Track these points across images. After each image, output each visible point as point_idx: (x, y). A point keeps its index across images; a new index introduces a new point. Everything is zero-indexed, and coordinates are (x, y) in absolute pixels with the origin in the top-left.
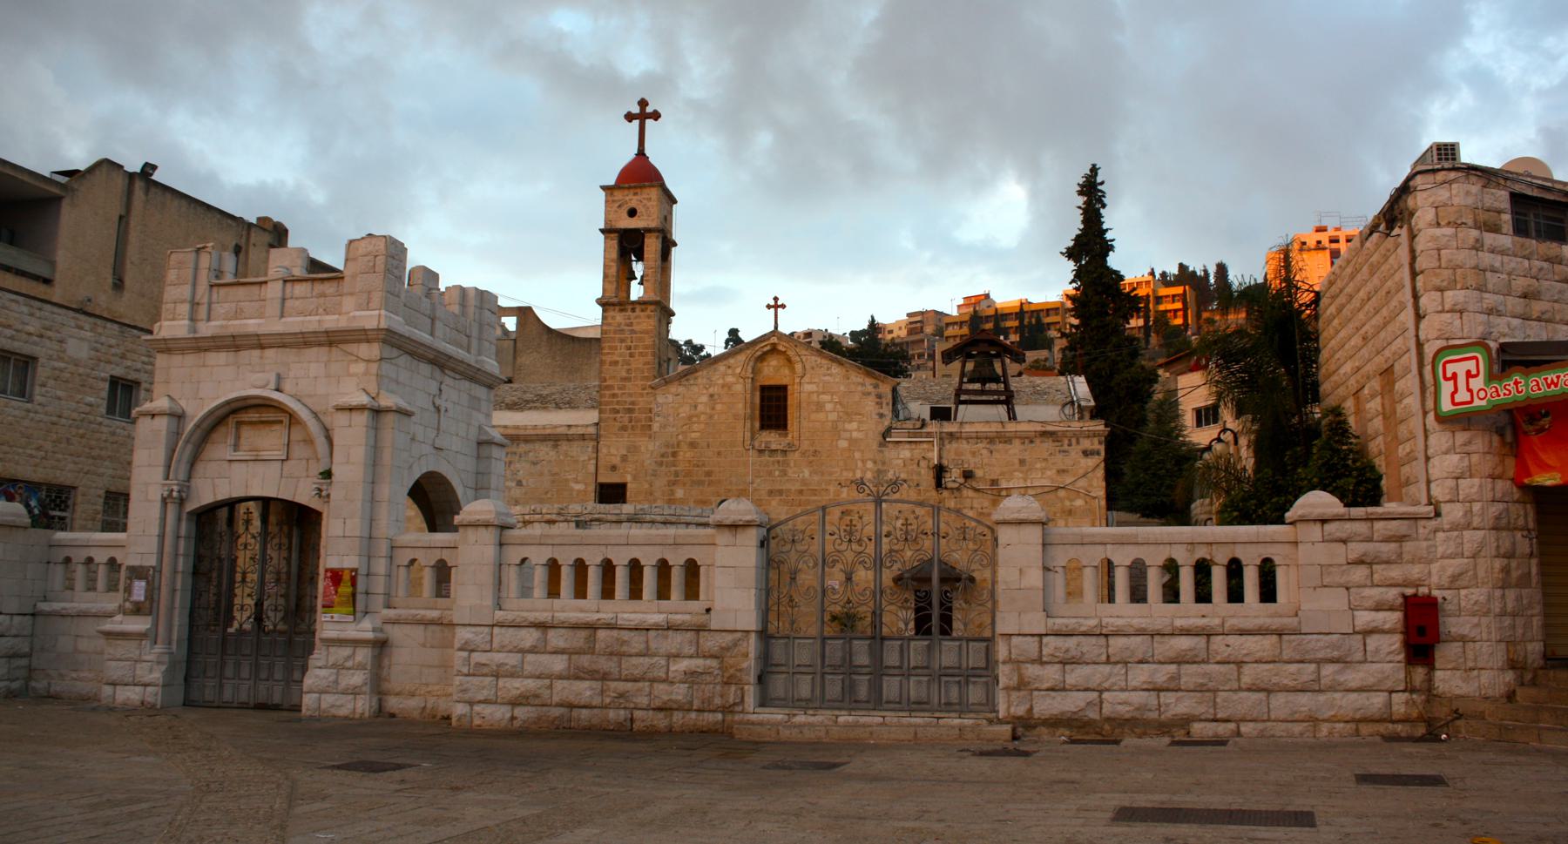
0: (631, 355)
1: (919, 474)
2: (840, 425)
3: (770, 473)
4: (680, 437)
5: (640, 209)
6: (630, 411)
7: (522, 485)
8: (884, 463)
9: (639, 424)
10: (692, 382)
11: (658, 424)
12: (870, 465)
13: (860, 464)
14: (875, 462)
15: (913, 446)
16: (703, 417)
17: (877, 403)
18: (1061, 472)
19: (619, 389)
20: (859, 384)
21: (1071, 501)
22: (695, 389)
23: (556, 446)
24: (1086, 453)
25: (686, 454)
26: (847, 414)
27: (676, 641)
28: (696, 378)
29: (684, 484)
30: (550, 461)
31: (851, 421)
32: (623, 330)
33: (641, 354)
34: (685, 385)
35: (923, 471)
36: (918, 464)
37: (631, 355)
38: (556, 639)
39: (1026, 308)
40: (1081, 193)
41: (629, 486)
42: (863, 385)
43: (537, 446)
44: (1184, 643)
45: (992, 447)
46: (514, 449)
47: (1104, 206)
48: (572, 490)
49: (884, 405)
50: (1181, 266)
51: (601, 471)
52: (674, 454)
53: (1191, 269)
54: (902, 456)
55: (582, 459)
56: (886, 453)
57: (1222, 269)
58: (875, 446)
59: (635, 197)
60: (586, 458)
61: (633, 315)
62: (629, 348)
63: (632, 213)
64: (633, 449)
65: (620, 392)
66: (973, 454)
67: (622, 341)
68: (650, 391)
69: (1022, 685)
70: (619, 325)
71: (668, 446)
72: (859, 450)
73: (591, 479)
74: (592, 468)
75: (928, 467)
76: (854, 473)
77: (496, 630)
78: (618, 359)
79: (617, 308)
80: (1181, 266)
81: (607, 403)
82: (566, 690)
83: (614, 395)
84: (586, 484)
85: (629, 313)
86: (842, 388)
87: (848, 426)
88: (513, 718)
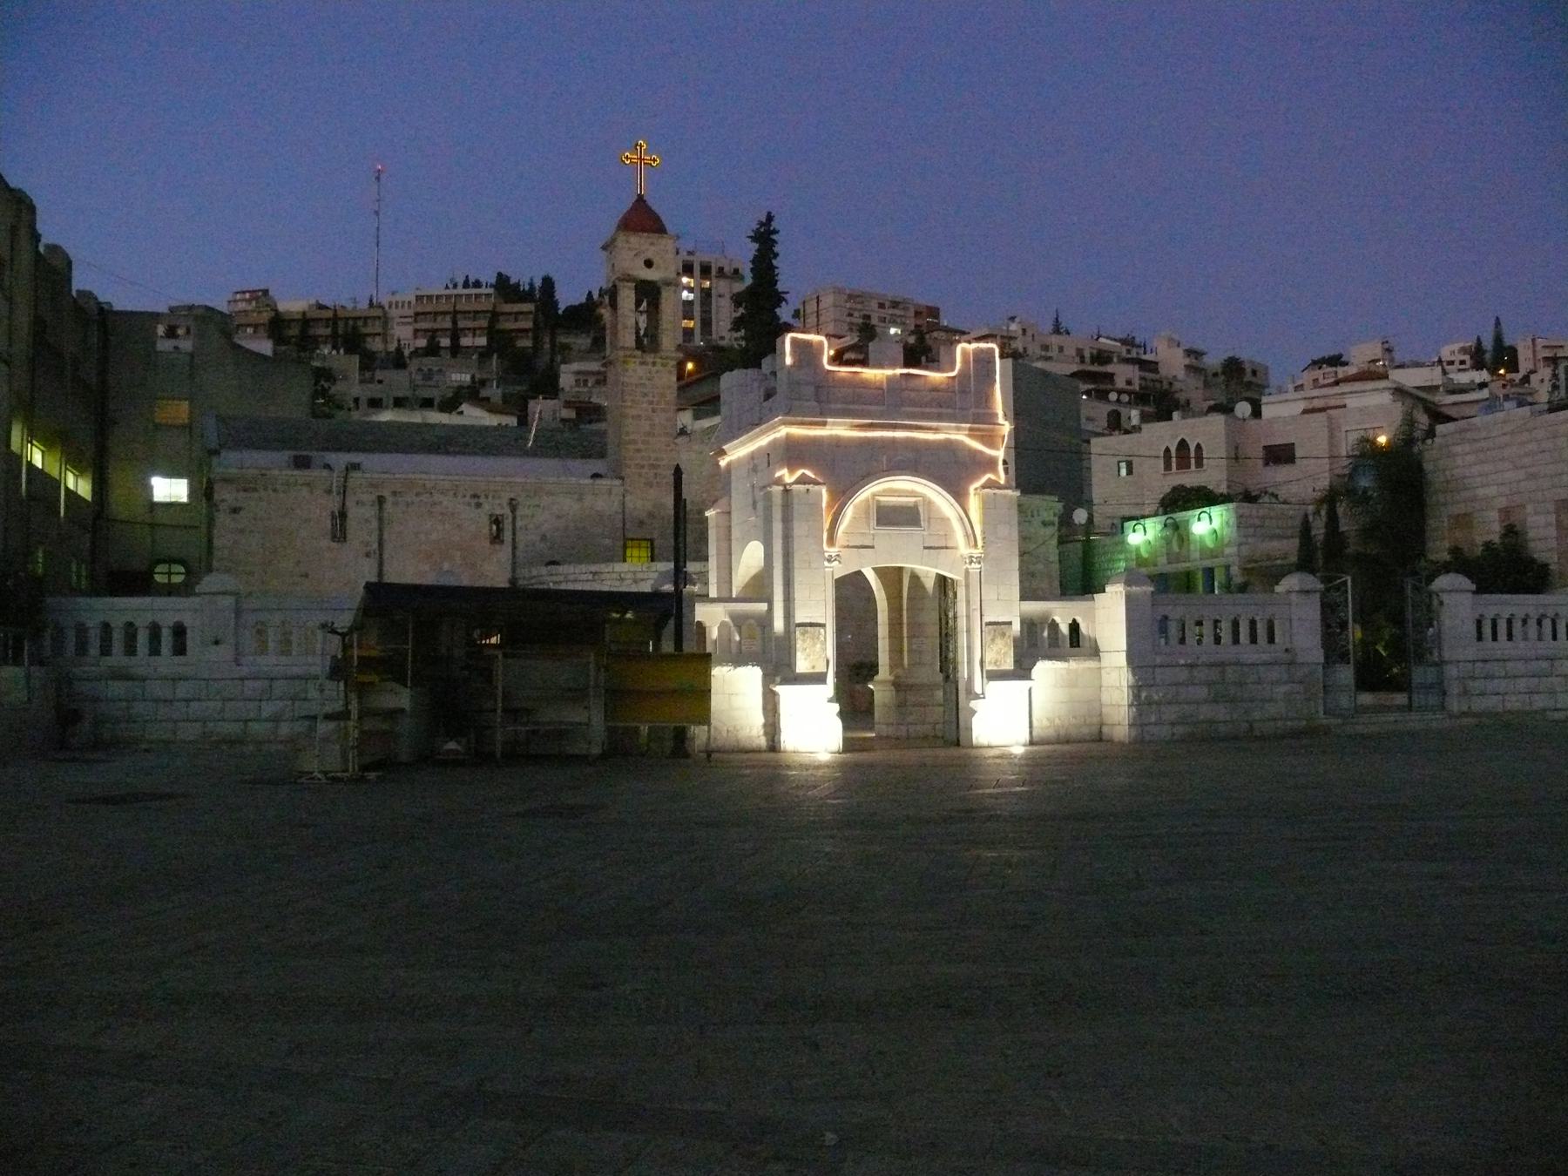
0: (654, 411)
4: (705, 495)
5: (656, 260)
6: (653, 466)
19: (644, 442)
24: (1045, 524)
27: (1274, 674)
32: (644, 384)
33: (663, 410)
37: (654, 411)
38: (1200, 674)
39: (341, 314)
40: (754, 239)
44: (1545, 664)
47: (776, 255)
50: (500, 274)
53: (513, 281)
57: (548, 283)
59: (653, 248)
62: (651, 403)
63: (649, 264)
69: (1465, 692)
70: (641, 378)
77: (1158, 670)
78: (640, 413)
80: (500, 274)
82: (1206, 712)
83: (638, 451)
85: (650, 367)
88: (1173, 734)
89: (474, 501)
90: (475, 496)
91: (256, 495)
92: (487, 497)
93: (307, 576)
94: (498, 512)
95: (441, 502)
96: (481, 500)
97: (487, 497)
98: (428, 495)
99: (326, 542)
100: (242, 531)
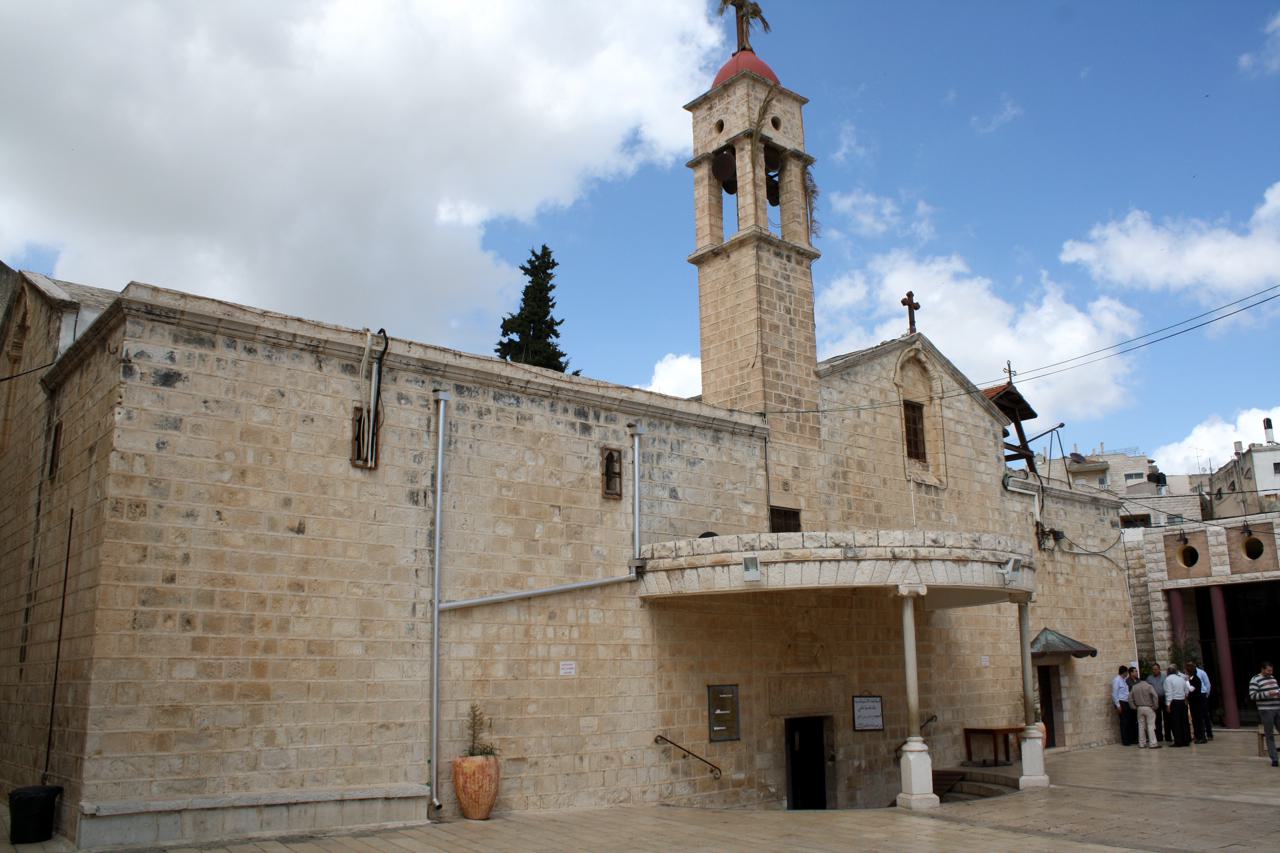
3: (928, 514)
4: (848, 452)
5: (784, 124)
7: (676, 497)
9: (807, 424)
10: (852, 378)
11: (826, 429)
16: (867, 429)
22: (857, 388)
23: (716, 440)
25: (855, 478)
28: (856, 374)
29: (858, 519)
30: (711, 463)
31: (980, 462)
32: (779, 283)
34: (846, 381)
37: (791, 321)
40: (527, 271)
41: (804, 516)
43: (693, 434)
46: (664, 435)
48: (740, 513)
51: (775, 487)
52: (845, 474)
55: (749, 466)
58: (998, 495)
60: (754, 465)
61: (789, 266)
62: (788, 311)
64: (804, 460)
65: (784, 373)
67: (781, 298)
68: (813, 378)
71: (837, 463)
73: (762, 500)
74: (761, 482)
76: (988, 524)
79: (772, 249)
81: (774, 386)
83: (778, 375)
84: (756, 506)
85: (785, 261)
89: (579, 421)
90: (582, 413)
91: (212, 354)
92: (597, 417)
93: (300, 530)
94: (614, 444)
95: (531, 418)
96: (591, 422)
97: (597, 417)
98: (512, 400)
99: (340, 464)
100: (176, 424)
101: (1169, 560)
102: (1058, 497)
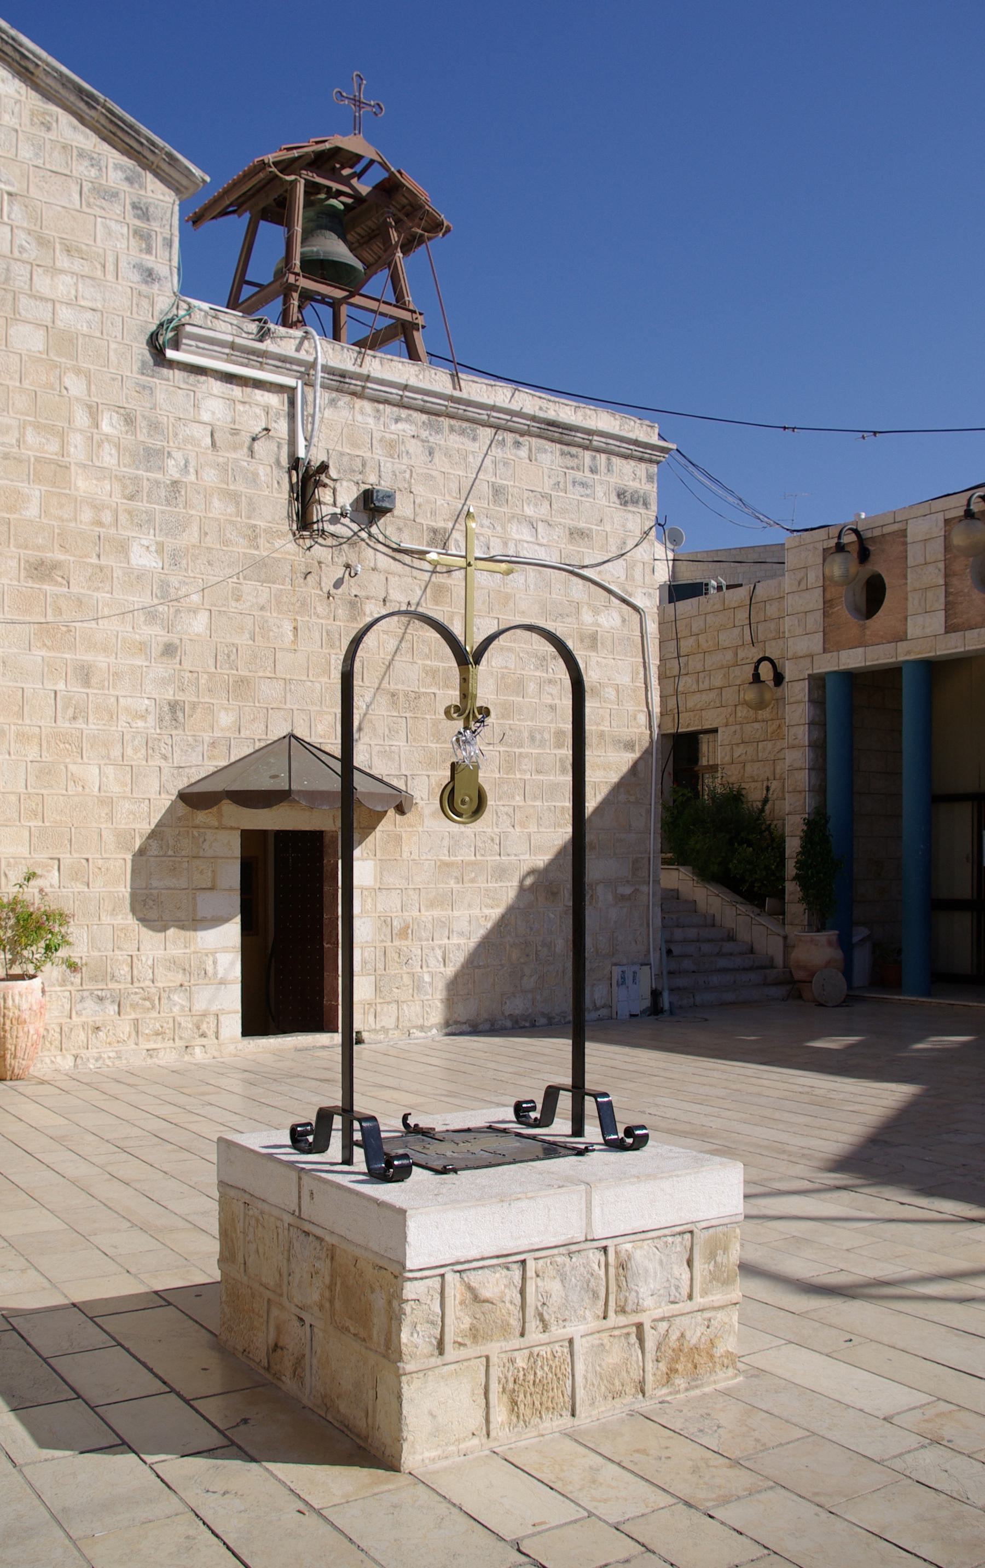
1: (253, 479)
2: (21, 271)
8: (154, 427)
12: (109, 425)
13: (81, 418)
14: (129, 420)
15: (236, 391)
17: (137, 233)
18: (577, 534)
20: (82, 154)
21: (596, 612)
24: (625, 498)
26: (43, 242)
31: (54, 271)
35: (262, 471)
36: (251, 450)
42: (94, 162)
45: (435, 439)
49: (158, 243)
54: (206, 417)
56: (160, 396)
66: (392, 447)
72: (78, 371)
75: (278, 462)
86: (26, 152)
87: (43, 284)
101: (828, 604)
102: (401, 405)
